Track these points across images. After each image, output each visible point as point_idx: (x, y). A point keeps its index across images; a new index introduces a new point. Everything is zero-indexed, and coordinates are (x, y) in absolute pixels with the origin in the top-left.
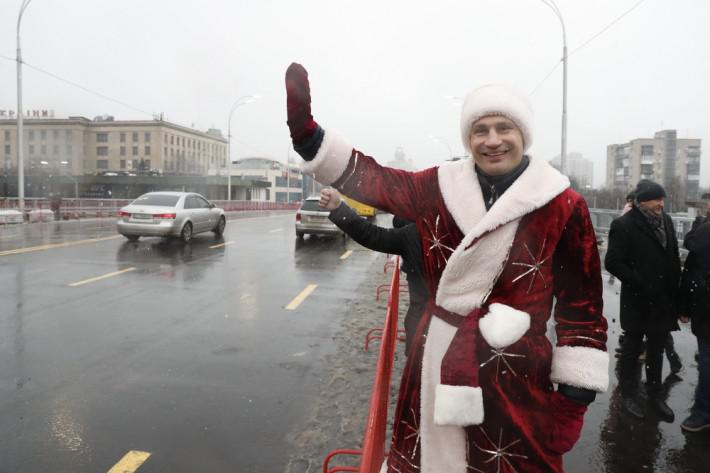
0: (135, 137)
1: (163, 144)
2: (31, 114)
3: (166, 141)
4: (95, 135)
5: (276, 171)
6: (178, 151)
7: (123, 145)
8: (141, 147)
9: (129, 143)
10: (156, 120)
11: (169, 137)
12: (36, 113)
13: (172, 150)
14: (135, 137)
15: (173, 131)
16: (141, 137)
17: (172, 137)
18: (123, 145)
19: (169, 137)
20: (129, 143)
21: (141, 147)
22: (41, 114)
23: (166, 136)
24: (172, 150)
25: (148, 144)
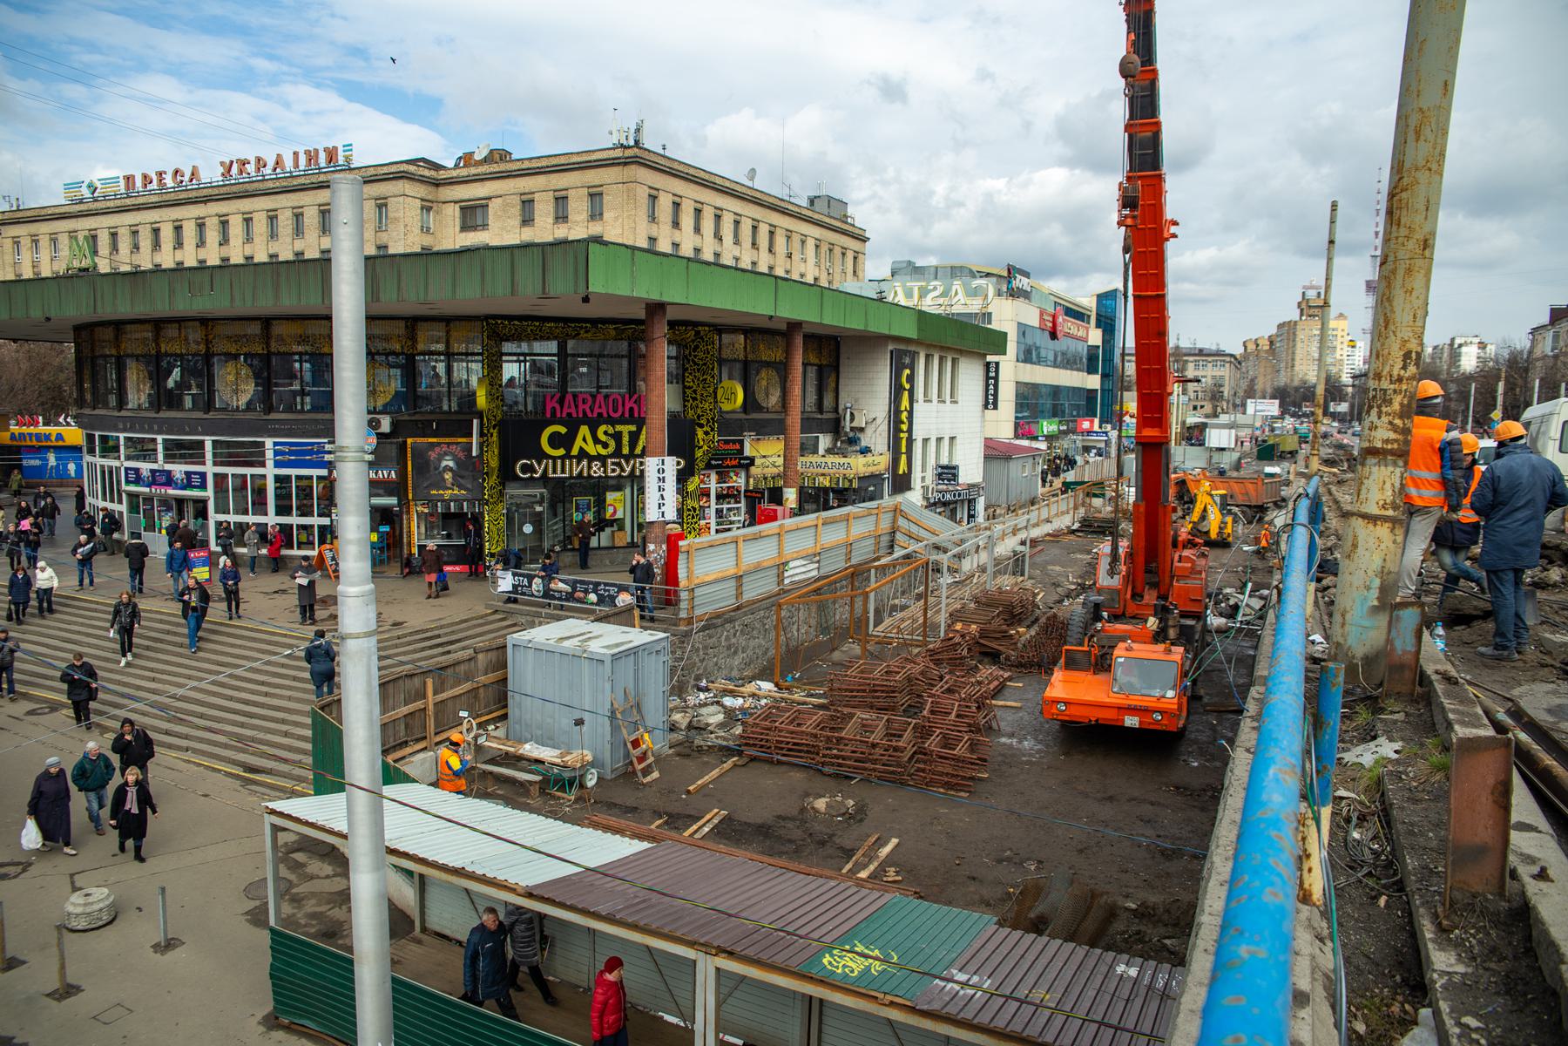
4: (453, 212)
5: (1020, 304)
12: (312, 156)
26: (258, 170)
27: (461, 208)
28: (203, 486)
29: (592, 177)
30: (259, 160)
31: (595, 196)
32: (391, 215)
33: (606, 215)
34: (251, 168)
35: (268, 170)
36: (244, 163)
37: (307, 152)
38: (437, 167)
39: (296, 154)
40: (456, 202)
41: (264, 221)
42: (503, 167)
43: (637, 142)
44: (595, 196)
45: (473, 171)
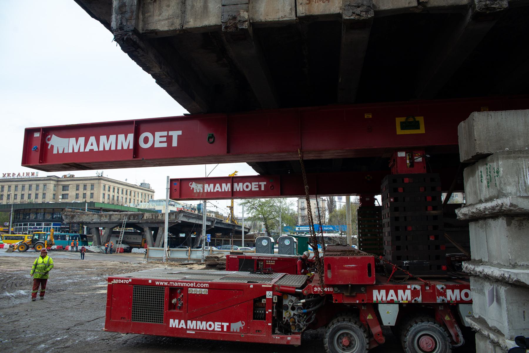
0: (85, 188)
1: (102, 192)
2: (25, 174)
3: (104, 190)
4: (61, 187)
6: (114, 196)
7: (77, 192)
8: (88, 193)
9: (81, 191)
10: (99, 176)
11: (107, 187)
13: (109, 195)
14: (85, 189)
15: (110, 183)
16: (89, 187)
17: (109, 187)
18: (77, 192)
19: (107, 187)
20: (81, 191)
21: (88, 193)
22: (30, 175)
23: (105, 186)
24: (109, 195)
25: (92, 192)
26: (13, 176)
27: (63, 186)
28: (42, 229)
29: (92, 182)
30: (13, 174)
31: (92, 185)
32: (47, 187)
33: (95, 189)
34: (11, 175)
35: (16, 176)
36: (9, 174)
37: (27, 173)
38: (58, 178)
39: (24, 173)
40: (62, 185)
41: (14, 187)
42: (72, 179)
43: (102, 175)
44: (92, 185)
45: (66, 179)
